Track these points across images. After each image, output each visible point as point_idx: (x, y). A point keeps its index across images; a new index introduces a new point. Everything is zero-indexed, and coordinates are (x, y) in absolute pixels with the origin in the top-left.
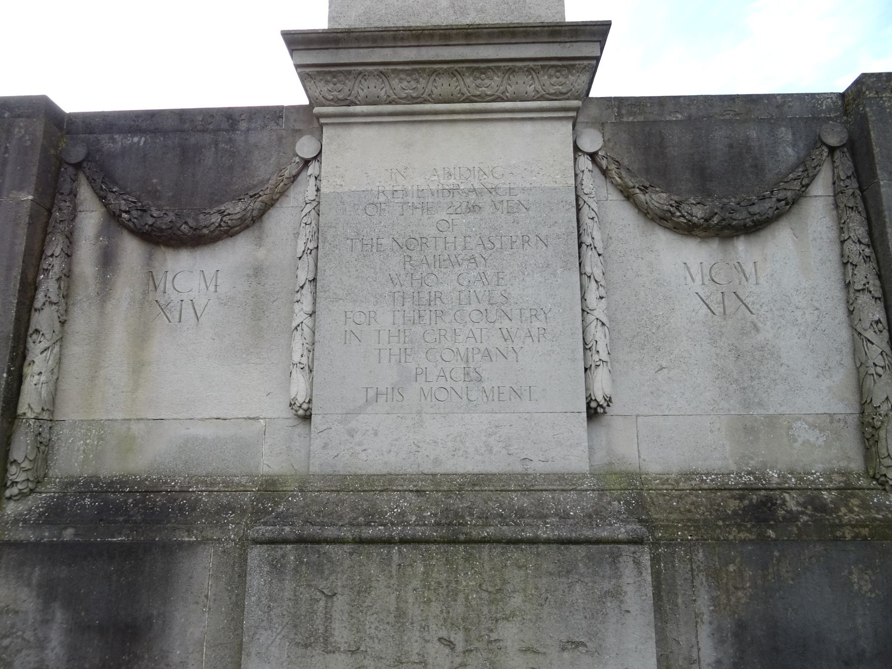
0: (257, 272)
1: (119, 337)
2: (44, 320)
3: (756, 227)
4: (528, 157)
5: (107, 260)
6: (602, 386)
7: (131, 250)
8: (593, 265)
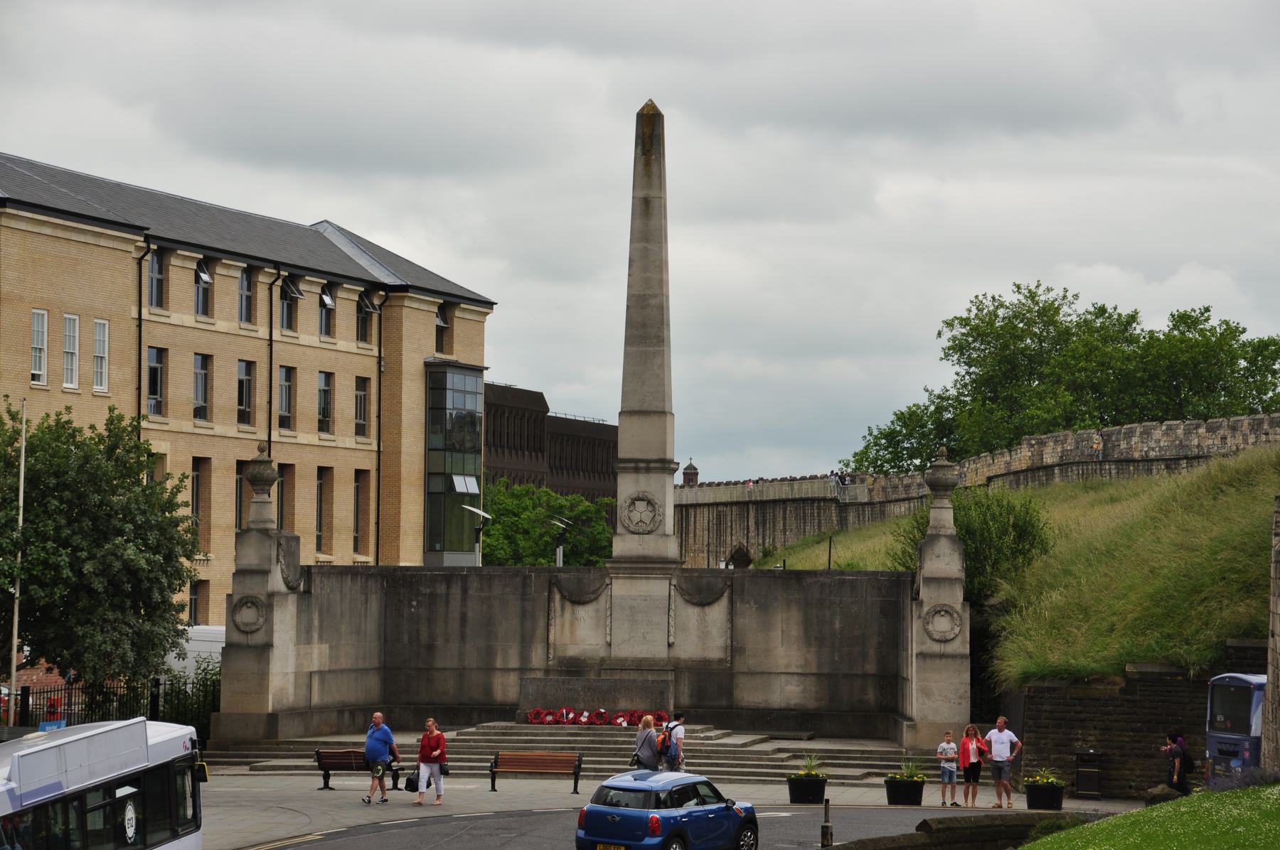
0: (597, 611)
1: (567, 625)
2: (552, 622)
3: (709, 604)
4: (658, 588)
5: (563, 608)
6: (672, 640)
7: (568, 605)
8: (672, 613)
